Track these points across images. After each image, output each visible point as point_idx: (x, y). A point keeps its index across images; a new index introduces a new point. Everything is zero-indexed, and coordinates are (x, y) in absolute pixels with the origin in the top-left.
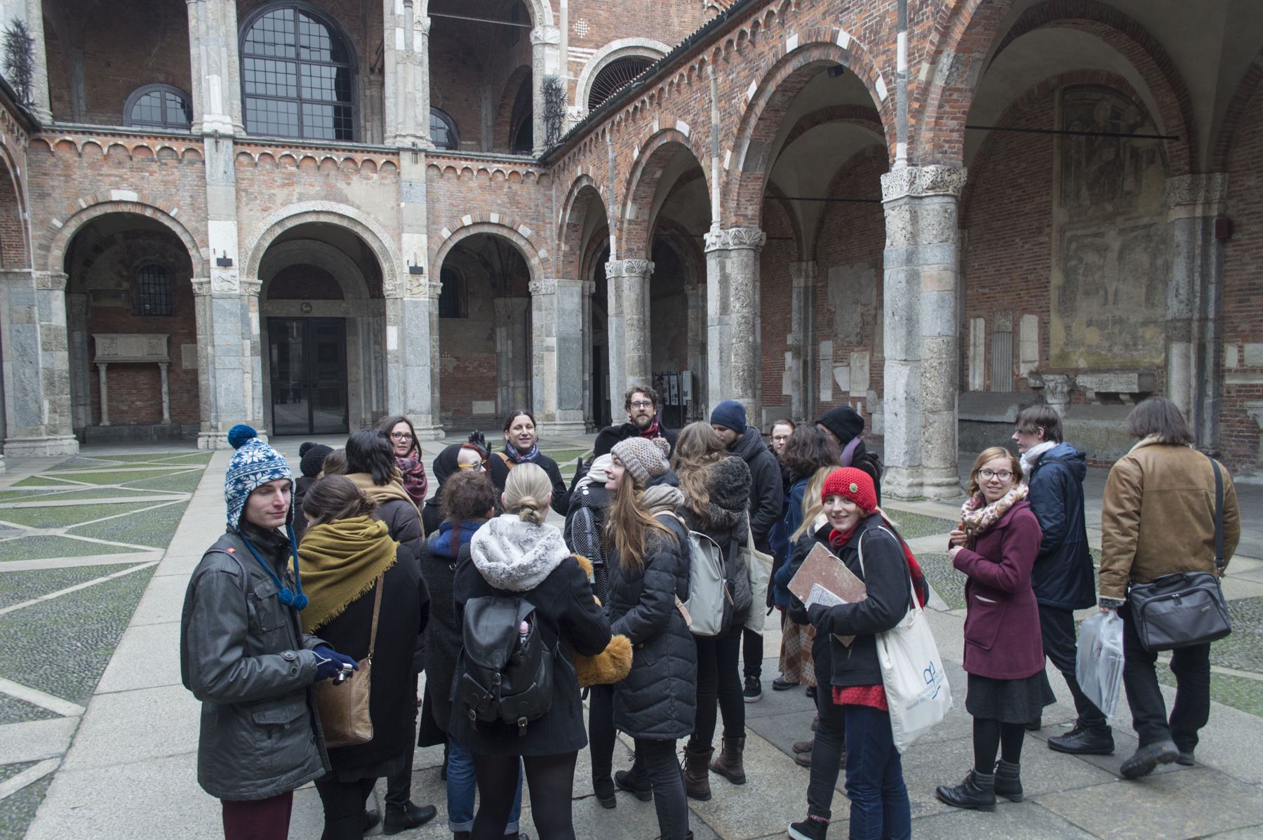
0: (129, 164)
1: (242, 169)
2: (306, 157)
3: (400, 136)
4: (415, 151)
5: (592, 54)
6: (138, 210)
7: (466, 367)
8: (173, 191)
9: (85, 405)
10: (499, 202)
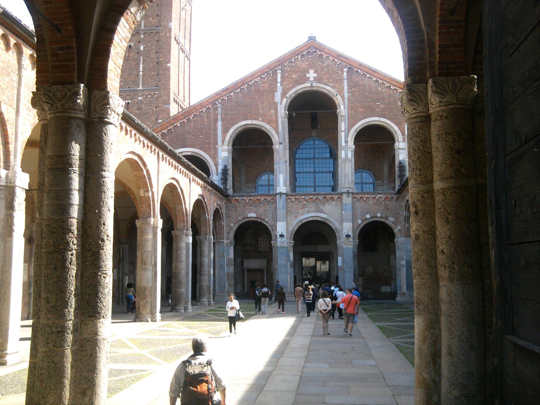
0: (254, 205)
1: (288, 204)
2: (310, 198)
3: (343, 188)
4: (348, 193)
6: (256, 219)
8: (267, 213)
10: (381, 209)
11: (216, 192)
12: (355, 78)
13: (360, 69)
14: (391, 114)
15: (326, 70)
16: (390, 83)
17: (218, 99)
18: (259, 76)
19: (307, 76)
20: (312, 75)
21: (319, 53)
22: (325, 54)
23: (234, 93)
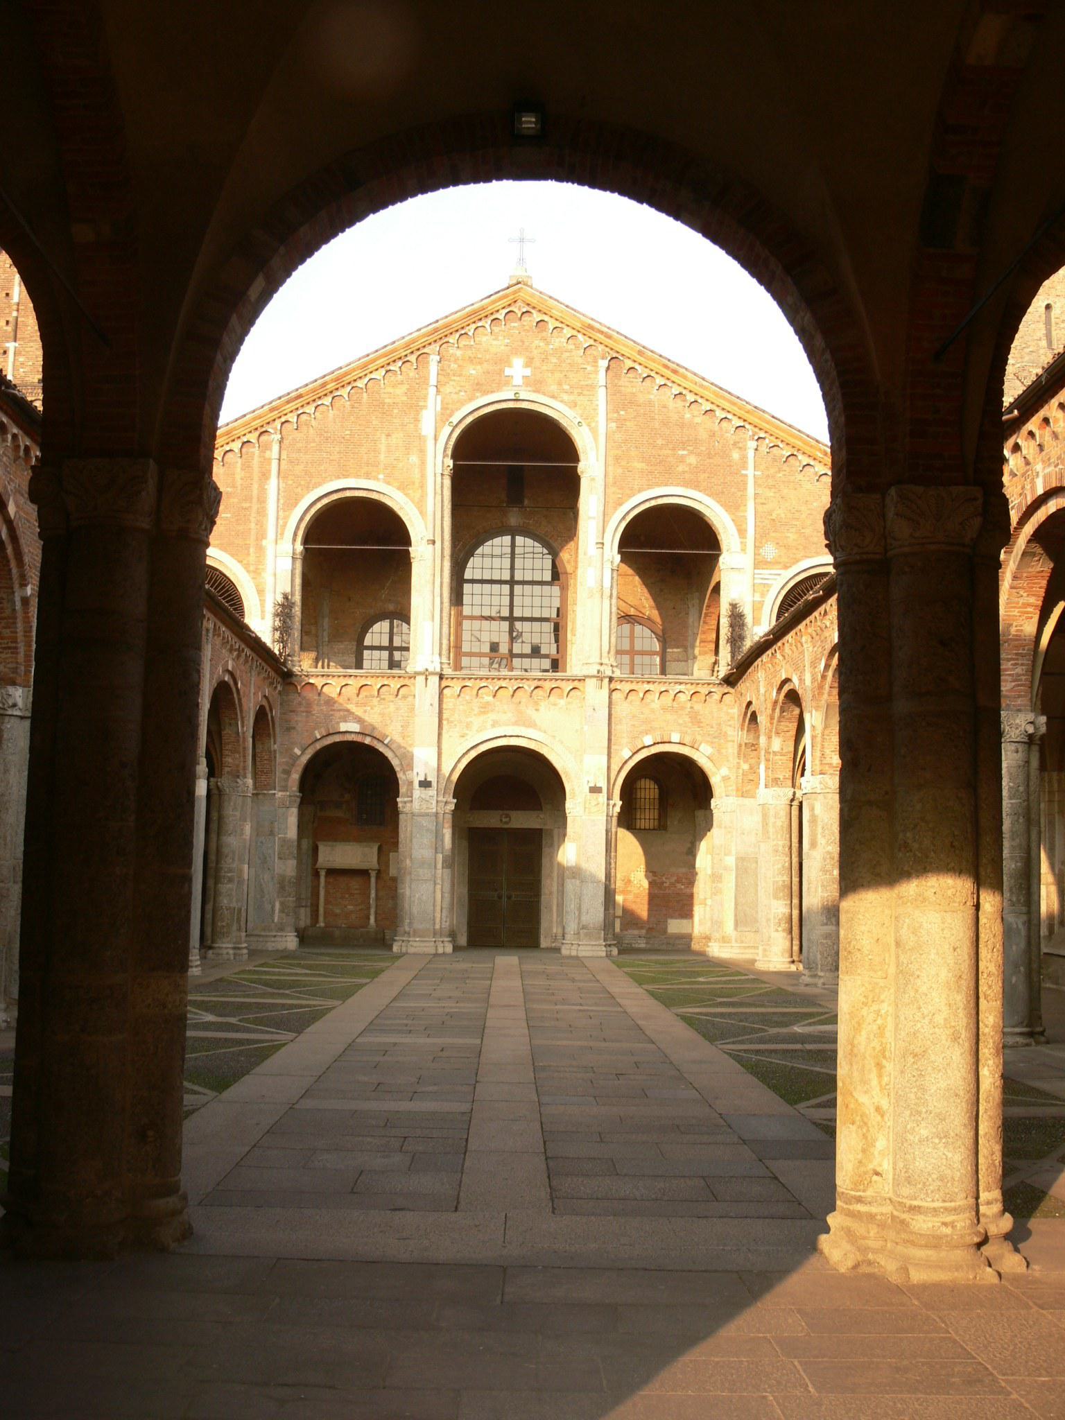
0: (355, 699)
4: (599, 677)
5: (779, 575)
6: (359, 739)
7: (663, 883)
9: (306, 906)
10: (681, 721)
11: (263, 664)
12: (627, 384)
13: (640, 364)
14: (713, 480)
15: (554, 360)
16: (712, 403)
17: (274, 420)
18: (383, 367)
19: (506, 374)
20: (517, 370)
21: (537, 317)
22: (553, 321)
23: (316, 408)
